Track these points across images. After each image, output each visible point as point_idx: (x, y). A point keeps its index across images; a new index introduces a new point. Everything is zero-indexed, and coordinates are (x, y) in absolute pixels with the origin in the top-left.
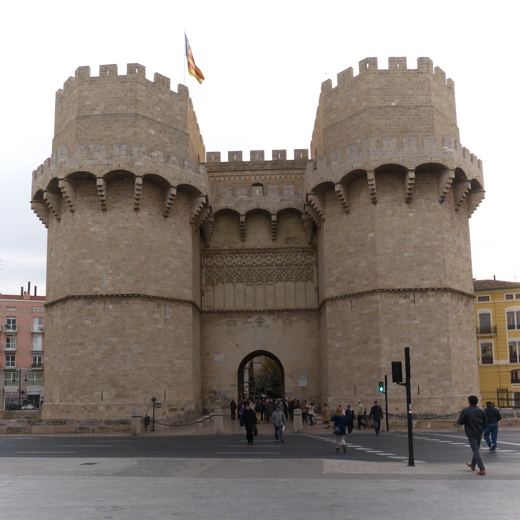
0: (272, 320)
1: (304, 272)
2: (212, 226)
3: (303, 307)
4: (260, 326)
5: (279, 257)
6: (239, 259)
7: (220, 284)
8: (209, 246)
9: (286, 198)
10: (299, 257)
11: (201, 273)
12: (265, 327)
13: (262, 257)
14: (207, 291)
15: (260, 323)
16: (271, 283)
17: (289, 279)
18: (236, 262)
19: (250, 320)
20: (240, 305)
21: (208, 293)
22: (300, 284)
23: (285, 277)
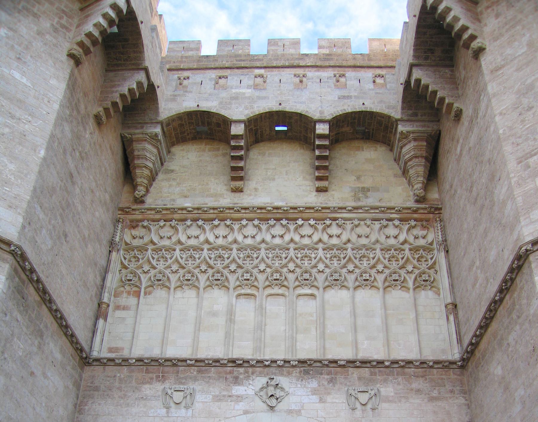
0: (314, 392)
1: (410, 268)
2: (155, 151)
3: (413, 355)
4: (272, 408)
5: (334, 230)
6: (222, 231)
7: (160, 293)
8: (140, 201)
9: (353, 94)
10: (391, 231)
11: (109, 261)
12: (290, 412)
13: (288, 230)
14: (118, 308)
15: (272, 399)
16: (309, 291)
17: (366, 283)
18: (211, 239)
19: (238, 390)
20: (212, 347)
21: (119, 314)
22: (398, 297)
23: (352, 277)
